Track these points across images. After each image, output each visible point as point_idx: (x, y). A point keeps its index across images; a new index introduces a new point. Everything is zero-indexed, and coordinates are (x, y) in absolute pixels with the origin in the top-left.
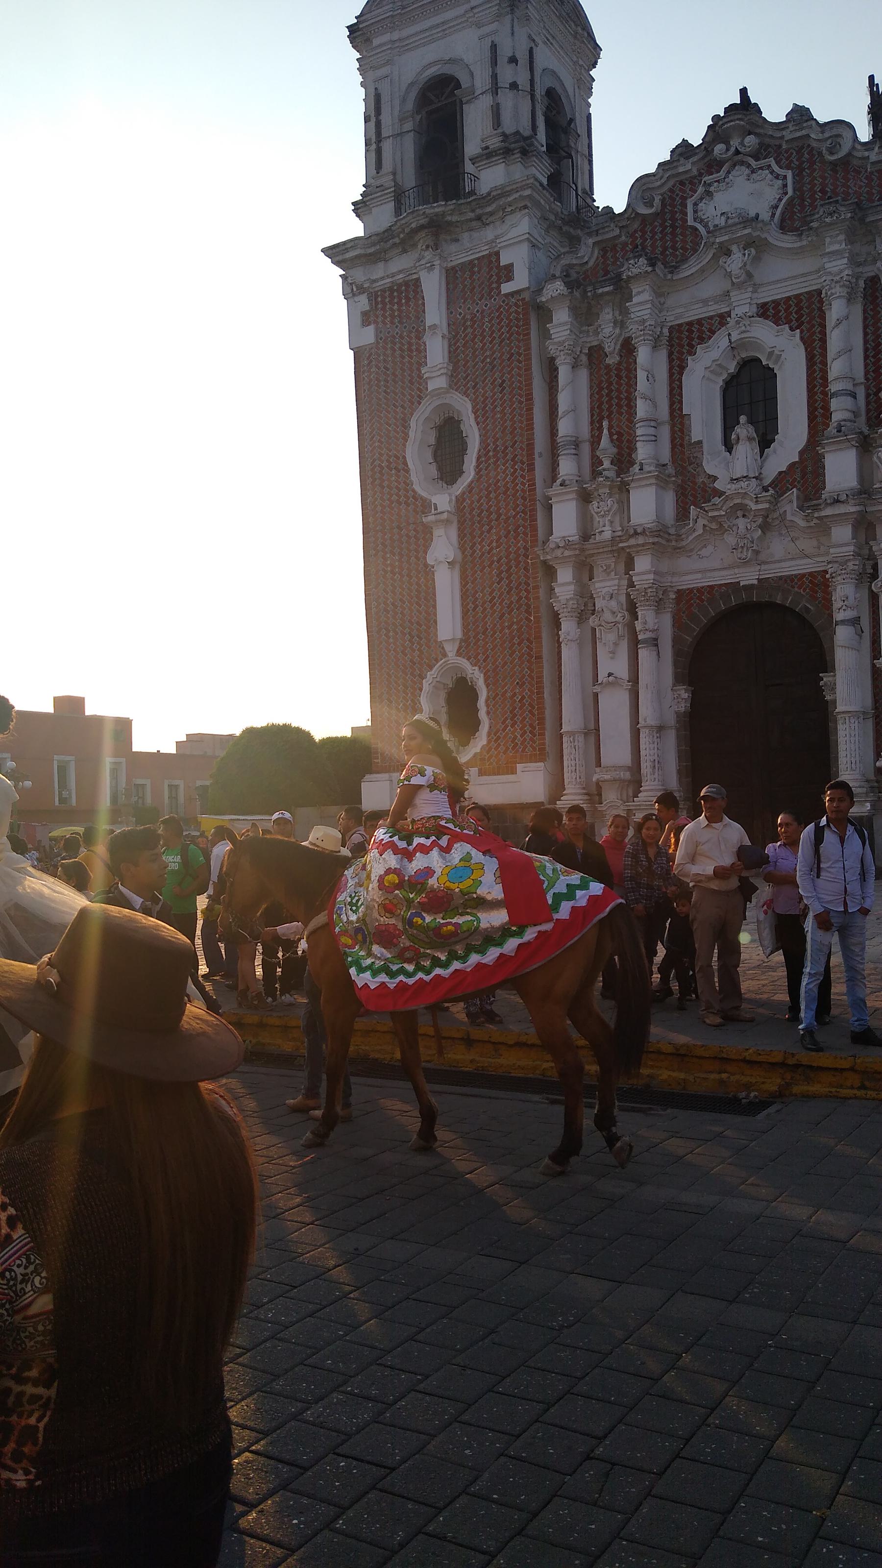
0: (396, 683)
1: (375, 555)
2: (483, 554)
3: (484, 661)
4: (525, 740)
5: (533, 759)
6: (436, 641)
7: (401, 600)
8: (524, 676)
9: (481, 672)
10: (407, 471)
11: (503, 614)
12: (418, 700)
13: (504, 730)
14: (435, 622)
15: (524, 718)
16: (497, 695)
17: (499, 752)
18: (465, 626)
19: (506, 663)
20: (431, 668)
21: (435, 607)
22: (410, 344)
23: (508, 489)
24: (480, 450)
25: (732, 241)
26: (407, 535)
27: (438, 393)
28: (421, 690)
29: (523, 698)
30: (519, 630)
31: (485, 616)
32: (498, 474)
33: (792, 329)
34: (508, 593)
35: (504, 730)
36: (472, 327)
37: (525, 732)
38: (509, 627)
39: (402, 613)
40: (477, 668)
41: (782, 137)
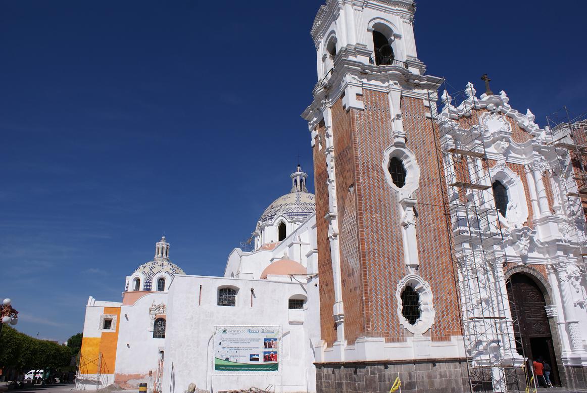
0: (380, 284)
1: (366, 211)
2: (425, 226)
3: (430, 279)
4: (454, 323)
5: (457, 334)
6: (403, 264)
7: (382, 238)
8: (450, 290)
9: (429, 284)
10: (384, 174)
11: (438, 258)
12: (394, 295)
13: (443, 317)
14: (403, 254)
15: (453, 312)
16: (438, 298)
17: (441, 329)
18: (420, 260)
19: (441, 282)
20: (401, 278)
21: (402, 246)
22: (382, 118)
23: (436, 198)
24: (420, 177)
25: (503, 137)
26: (384, 205)
27: (397, 145)
28: (396, 290)
29: (451, 301)
30: (447, 266)
31: (429, 256)
32: (430, 190)
33: (518, 174)
34: (440, 247)
35: (443, 317)
36: (413, 123)
37: (453, 319)
38: (442, 264)
39: (383, 245)
40: (427, 282)
41: (506, 112)
